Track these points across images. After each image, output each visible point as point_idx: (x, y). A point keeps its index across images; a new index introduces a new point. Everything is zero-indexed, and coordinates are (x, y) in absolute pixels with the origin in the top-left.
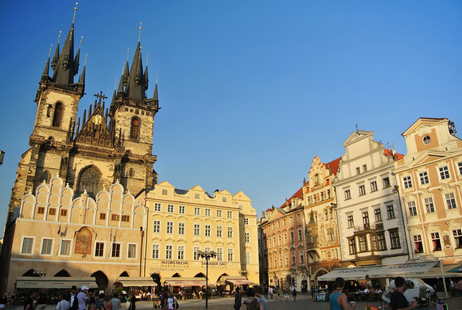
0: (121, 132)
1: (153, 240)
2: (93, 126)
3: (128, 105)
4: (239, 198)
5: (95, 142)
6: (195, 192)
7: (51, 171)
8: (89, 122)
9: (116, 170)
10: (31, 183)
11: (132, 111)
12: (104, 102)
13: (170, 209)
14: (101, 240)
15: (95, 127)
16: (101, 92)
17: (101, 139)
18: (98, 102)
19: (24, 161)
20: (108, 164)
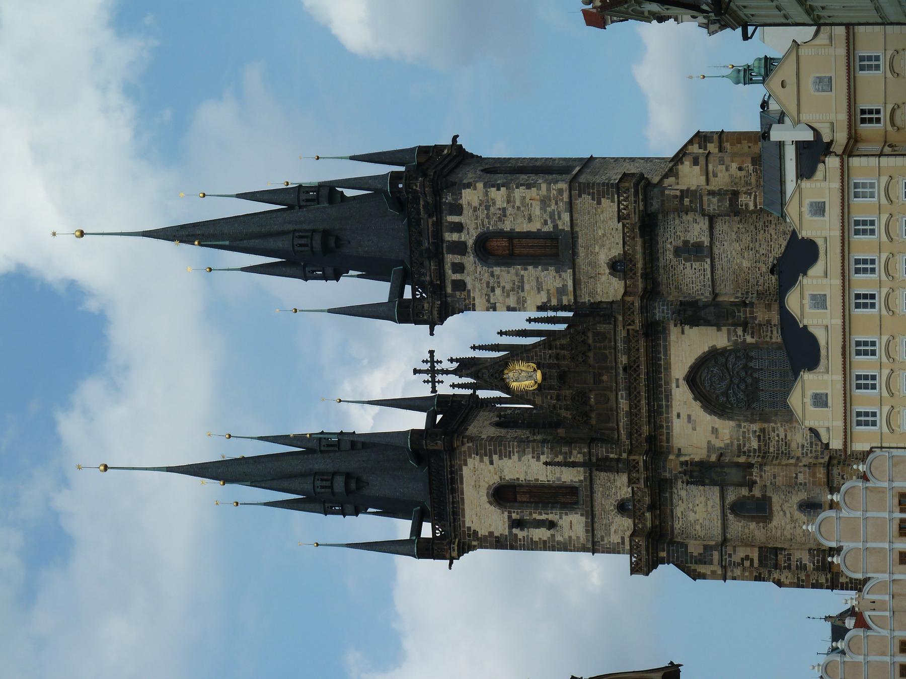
2: (551, 388)
3: (442, 287)
4: (791, 88)
5: (605, 378)
6: (807, 310)
7: (731, 497)
8: (538, 400)
9: (695, 321)
10: (780, 557)
11: (459, 268)
12: (451, 360)
13: (867, 382)
15: (554, 382)
16: (416, 371)
17: (591, 361)
18: (457, 380)
19: (713, 572)
20: (674, 332)
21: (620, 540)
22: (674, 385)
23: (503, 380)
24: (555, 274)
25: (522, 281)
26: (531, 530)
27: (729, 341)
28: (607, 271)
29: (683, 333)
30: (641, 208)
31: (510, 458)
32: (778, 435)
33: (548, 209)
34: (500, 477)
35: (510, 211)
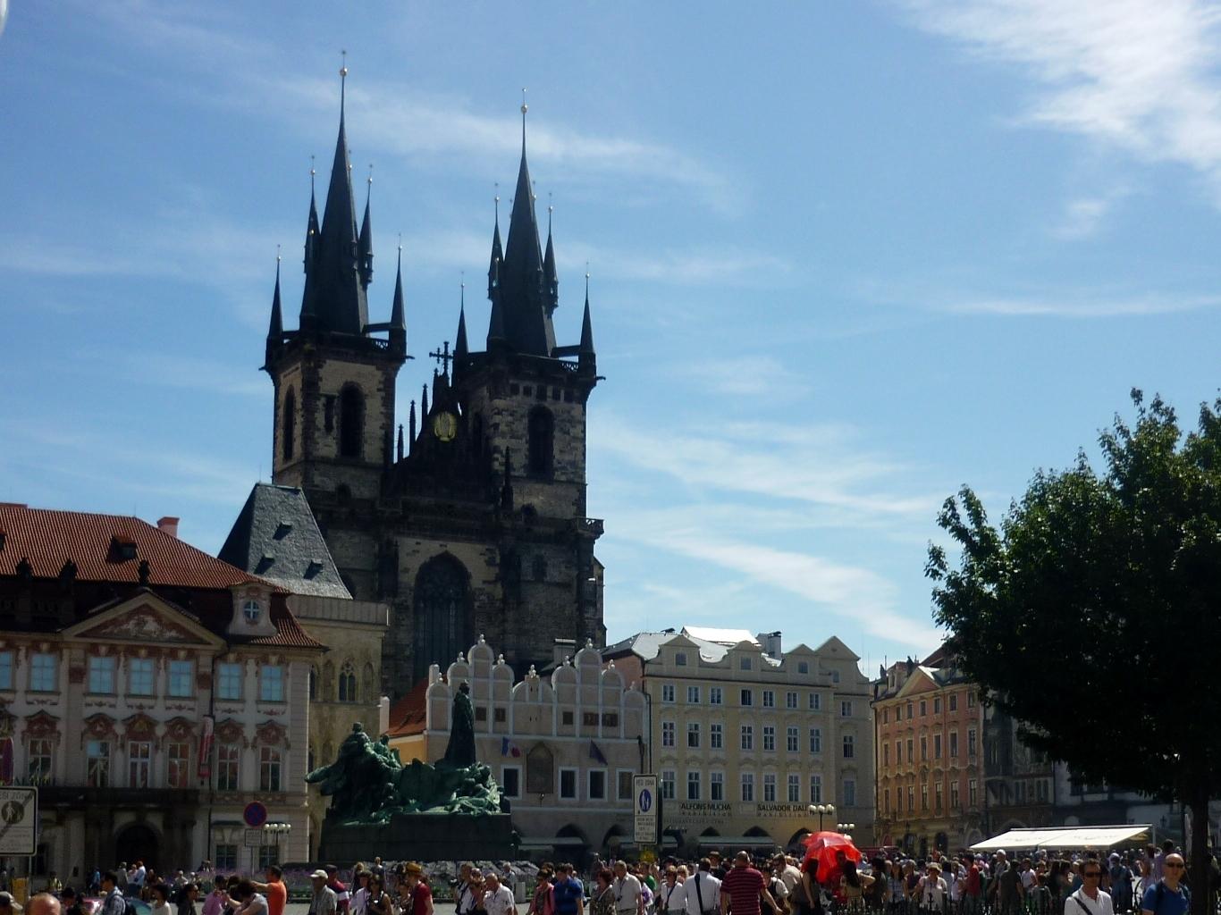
0: (507, 457)
1: (662, 761)
11: (527, 392)
14: (570, 765)
16: (446, 344)
18: (441, 373)
20: (481, 547)
21: (316, 483)
22: (441, 542)
23: (443, 411)
24: (523, 463)
25: (518, 438)
26: (323, 413)
27: (476, 589)
28: (525, 503)
29: (481, 554)
30: (586, 536)
31: (383, 405)
32: (403, 619)
33: (568, 467)
34: (366, 395)
35: (567, 437)
